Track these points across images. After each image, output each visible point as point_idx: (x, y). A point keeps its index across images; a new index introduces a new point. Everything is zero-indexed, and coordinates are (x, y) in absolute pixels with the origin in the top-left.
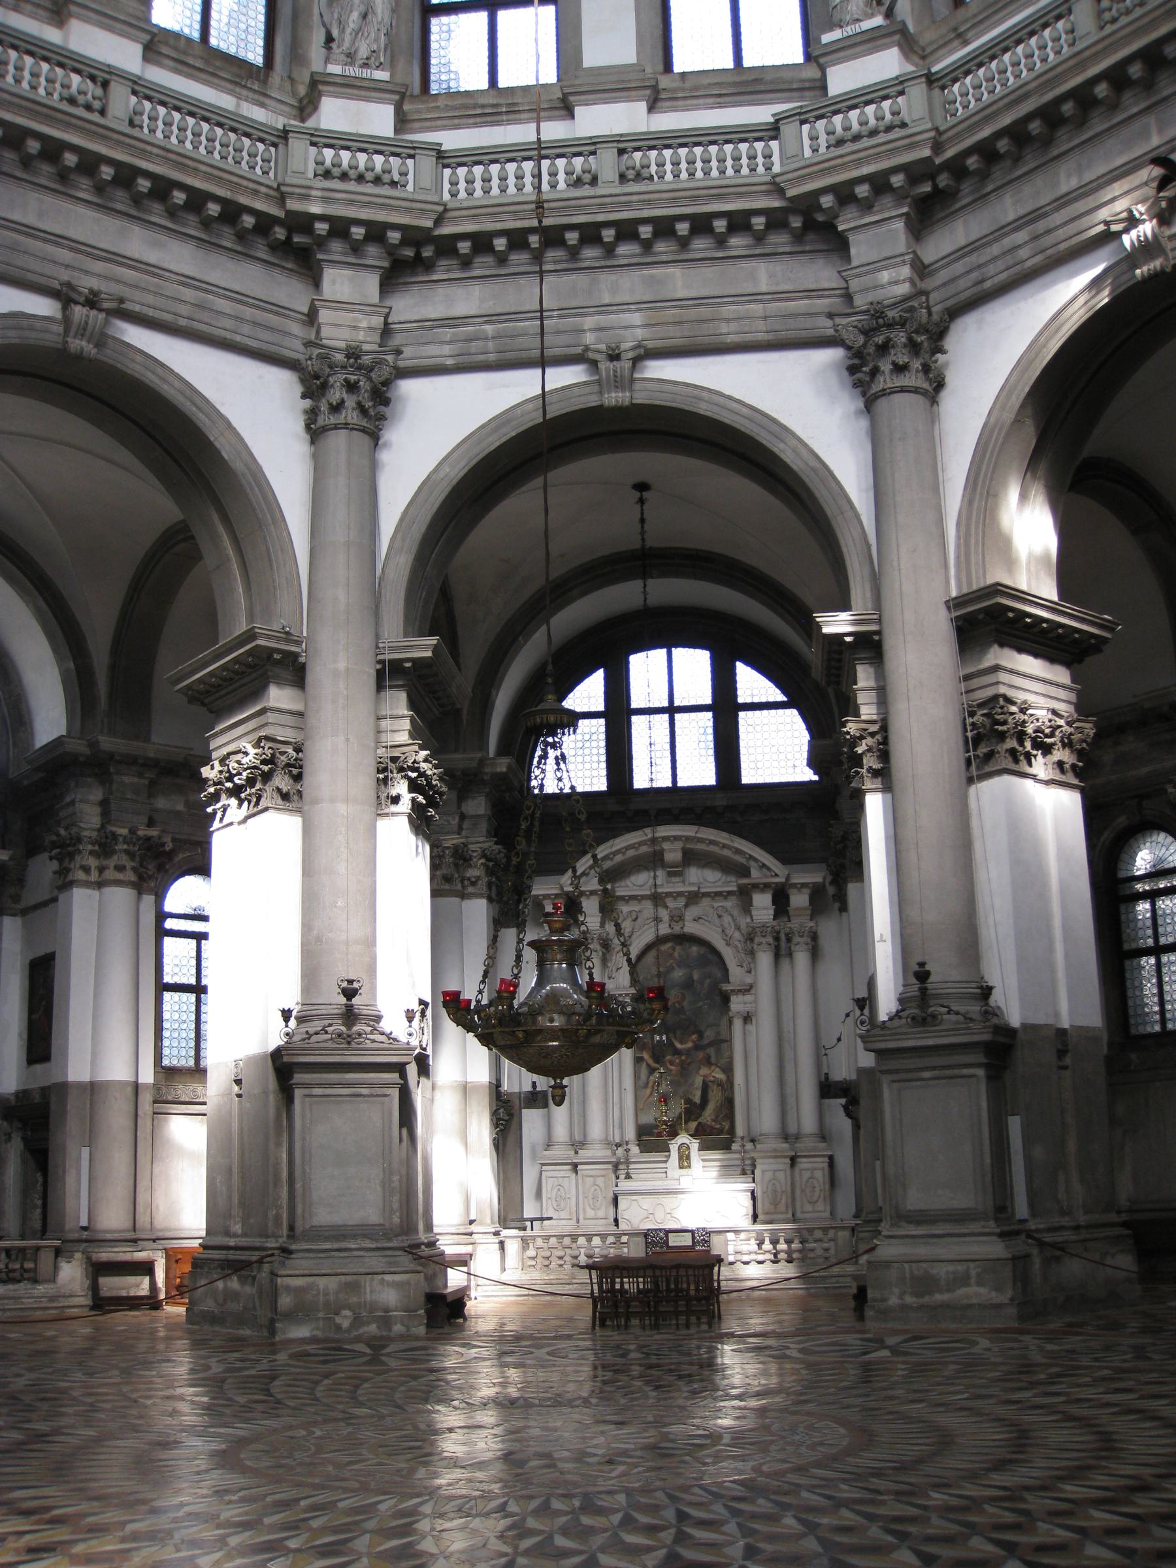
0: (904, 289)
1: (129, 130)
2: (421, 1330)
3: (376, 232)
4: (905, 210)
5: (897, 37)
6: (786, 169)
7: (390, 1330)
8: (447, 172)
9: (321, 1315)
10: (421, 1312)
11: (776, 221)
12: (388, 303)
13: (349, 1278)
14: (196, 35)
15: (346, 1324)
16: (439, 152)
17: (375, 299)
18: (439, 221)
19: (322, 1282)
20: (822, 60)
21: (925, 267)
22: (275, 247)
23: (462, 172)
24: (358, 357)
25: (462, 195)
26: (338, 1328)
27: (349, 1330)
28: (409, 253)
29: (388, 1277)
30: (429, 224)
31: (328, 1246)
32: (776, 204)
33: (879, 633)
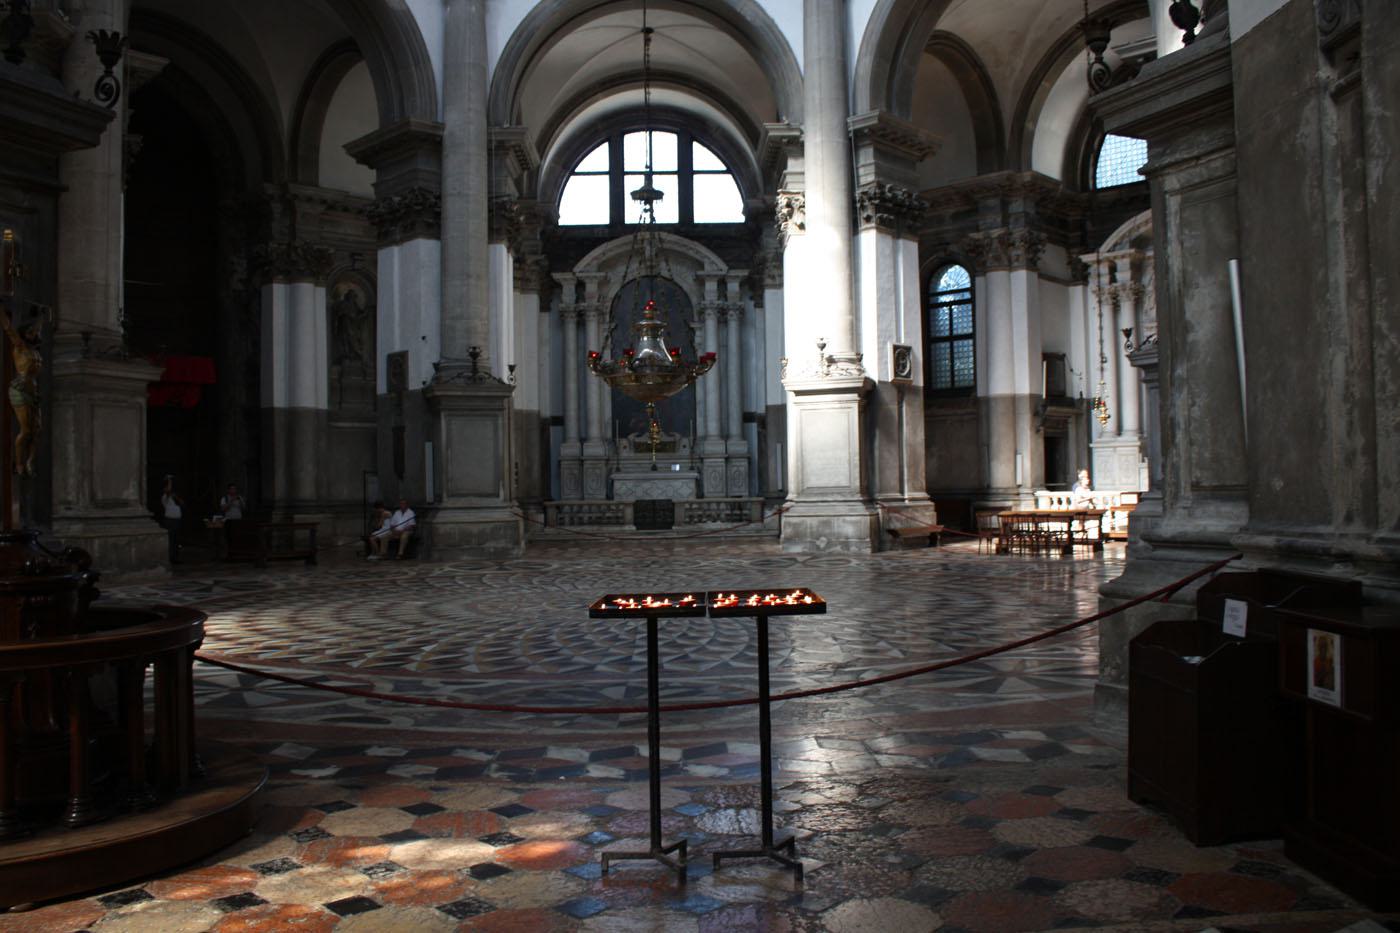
2: (868, 551)
7: (848, 549)
9: (809, 539)
10: (868, 540)
13: (825, 519)
15: (822, 545)
19: (808, 520)
26: (818, 548)
27: (824, 549)
29: (848, 518)
31: (815, 499)
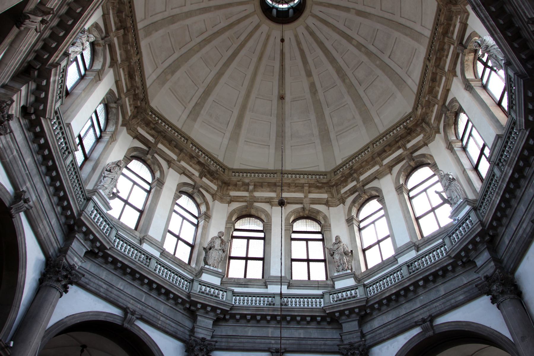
1: (154, 271)
3: (214, 309)
5: (353, 275)
6: (325, 306)
8: (234, 297)
11: (323, 318)
12: (214, 329)
14: (173, 253)
16: (233, 291)
17: (211, 327)
18: (231, 309)
20: (334, 280)
21: (364, 334)
22: (185, 309)
23: (238, 298)
24: (204, 342)
25: (237, 304)
28: (222, 316)
30: (228, 309)
32: (322, 314)
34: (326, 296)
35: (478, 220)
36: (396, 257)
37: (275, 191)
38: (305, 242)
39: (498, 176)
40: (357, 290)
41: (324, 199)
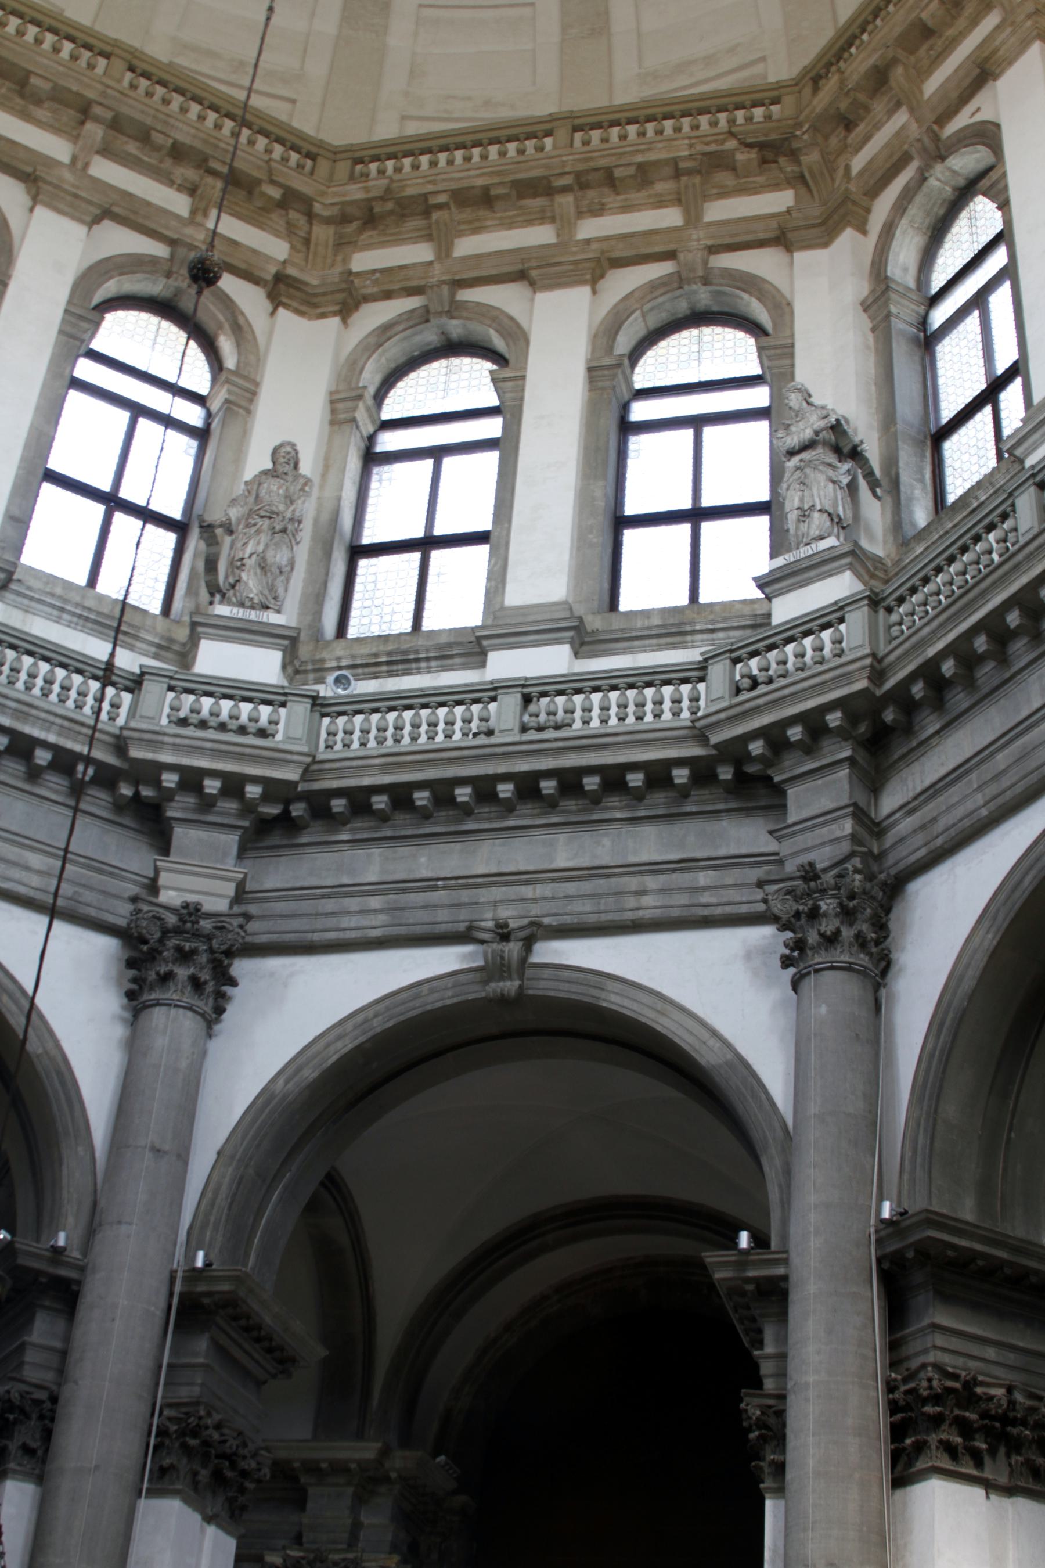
0: (221, 905)
4: (246, 823)
6: (133, 724)
33: (79, 1283)
34: (152, 689)
35: (867, 651)
36: (485, 643)
37: (75, 139)
38: (123, 416)
39: (1022, 529)
40: (282, 711)
41: (268, 258)
